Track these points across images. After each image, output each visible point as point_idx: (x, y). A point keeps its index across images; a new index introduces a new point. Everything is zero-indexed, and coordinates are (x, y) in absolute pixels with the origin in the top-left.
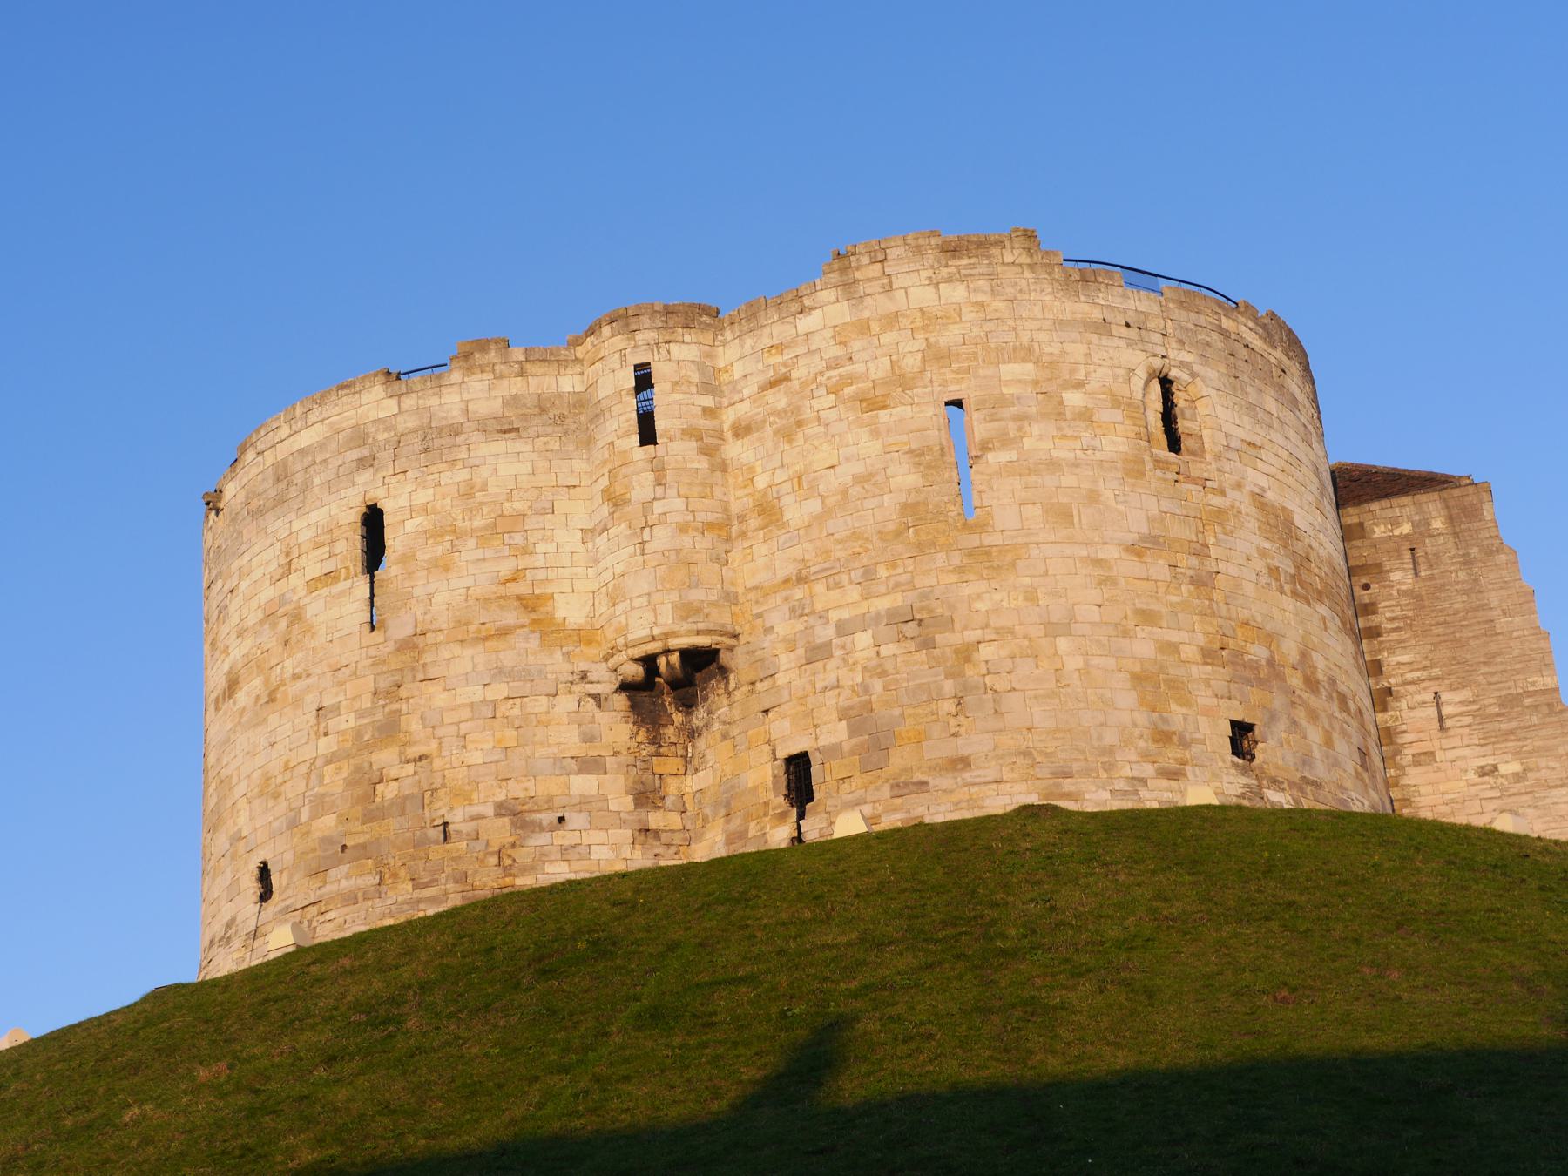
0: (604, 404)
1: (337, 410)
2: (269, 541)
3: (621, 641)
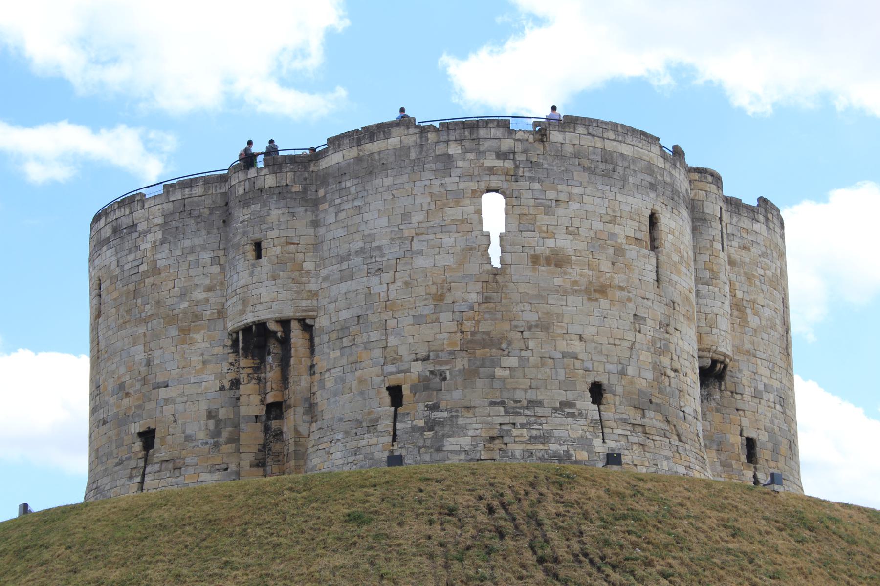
0: (708, 217)
1: (640, 145)
2: (600, 195)
3: (714, 348)
